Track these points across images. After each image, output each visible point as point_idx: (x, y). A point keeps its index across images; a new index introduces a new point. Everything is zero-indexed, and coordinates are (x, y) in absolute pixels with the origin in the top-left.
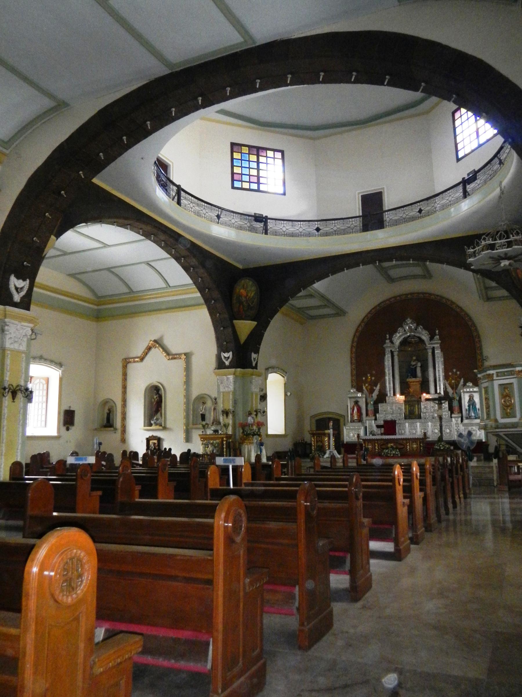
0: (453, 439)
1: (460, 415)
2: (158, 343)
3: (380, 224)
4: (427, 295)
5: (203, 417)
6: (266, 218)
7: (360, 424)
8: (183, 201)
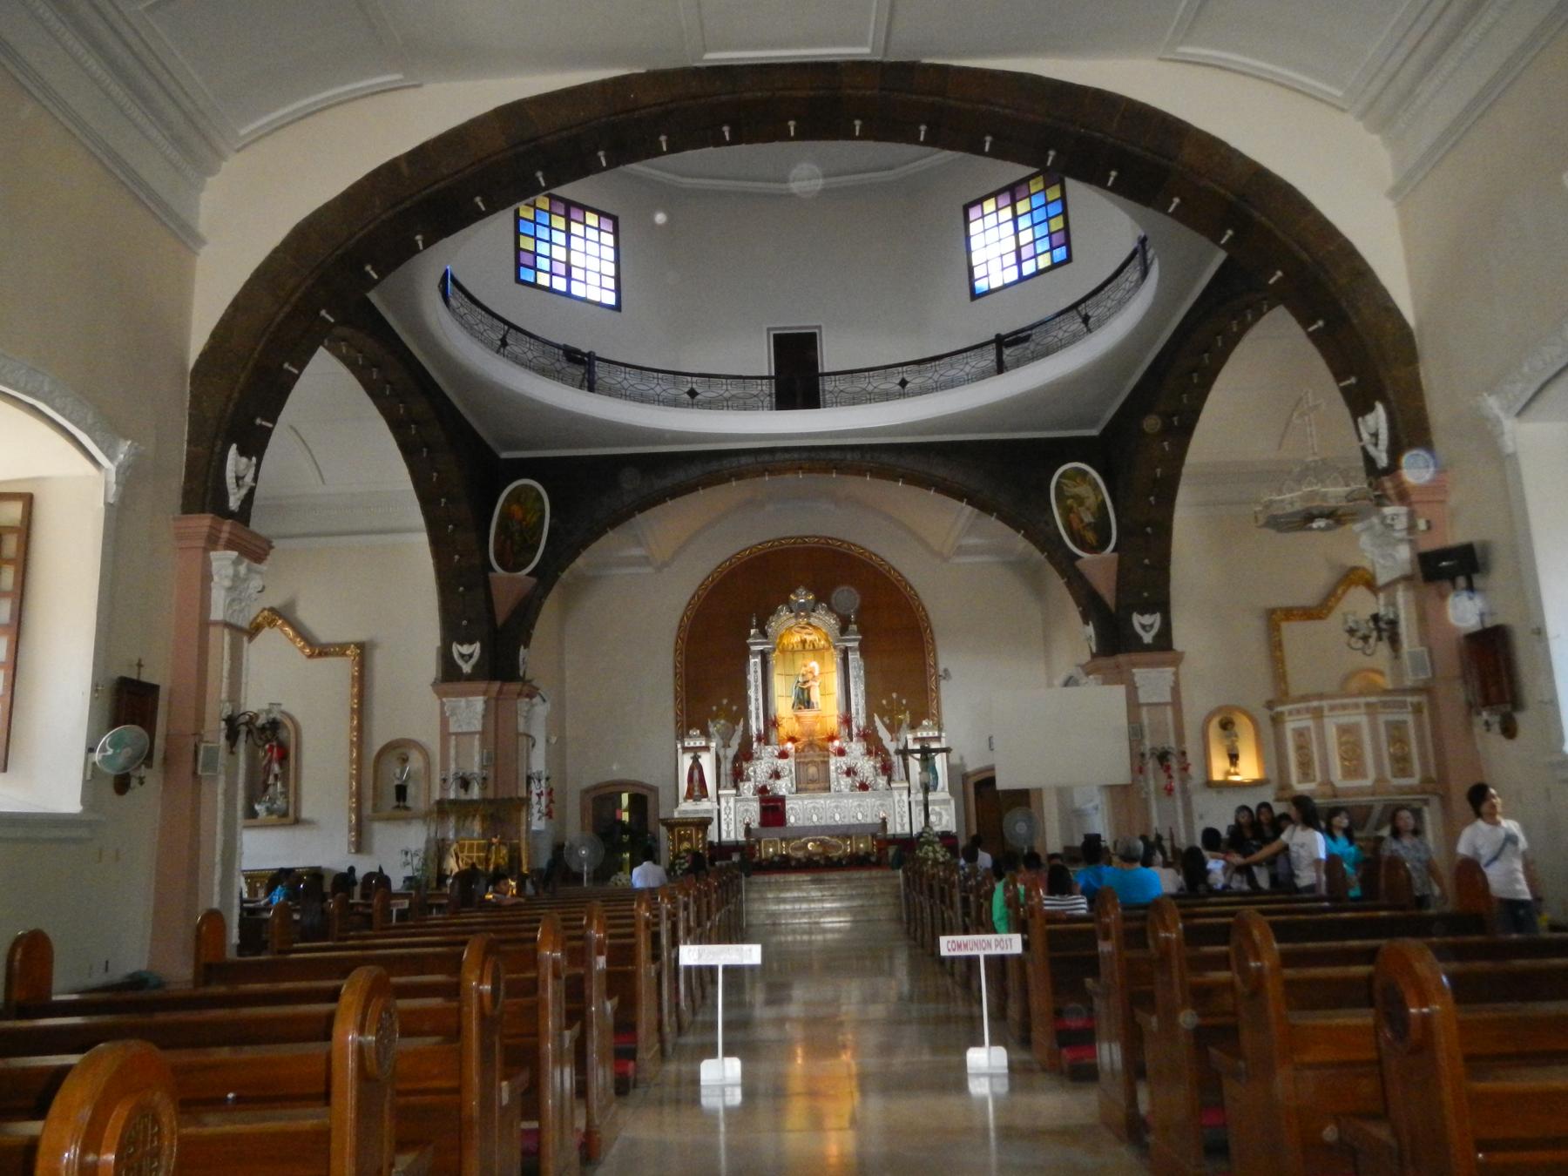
2: (282, 615)
3: (811, 400)
5: (401, 792)
6: (590, 355)
7: (705, 805)
8: (453, 302)
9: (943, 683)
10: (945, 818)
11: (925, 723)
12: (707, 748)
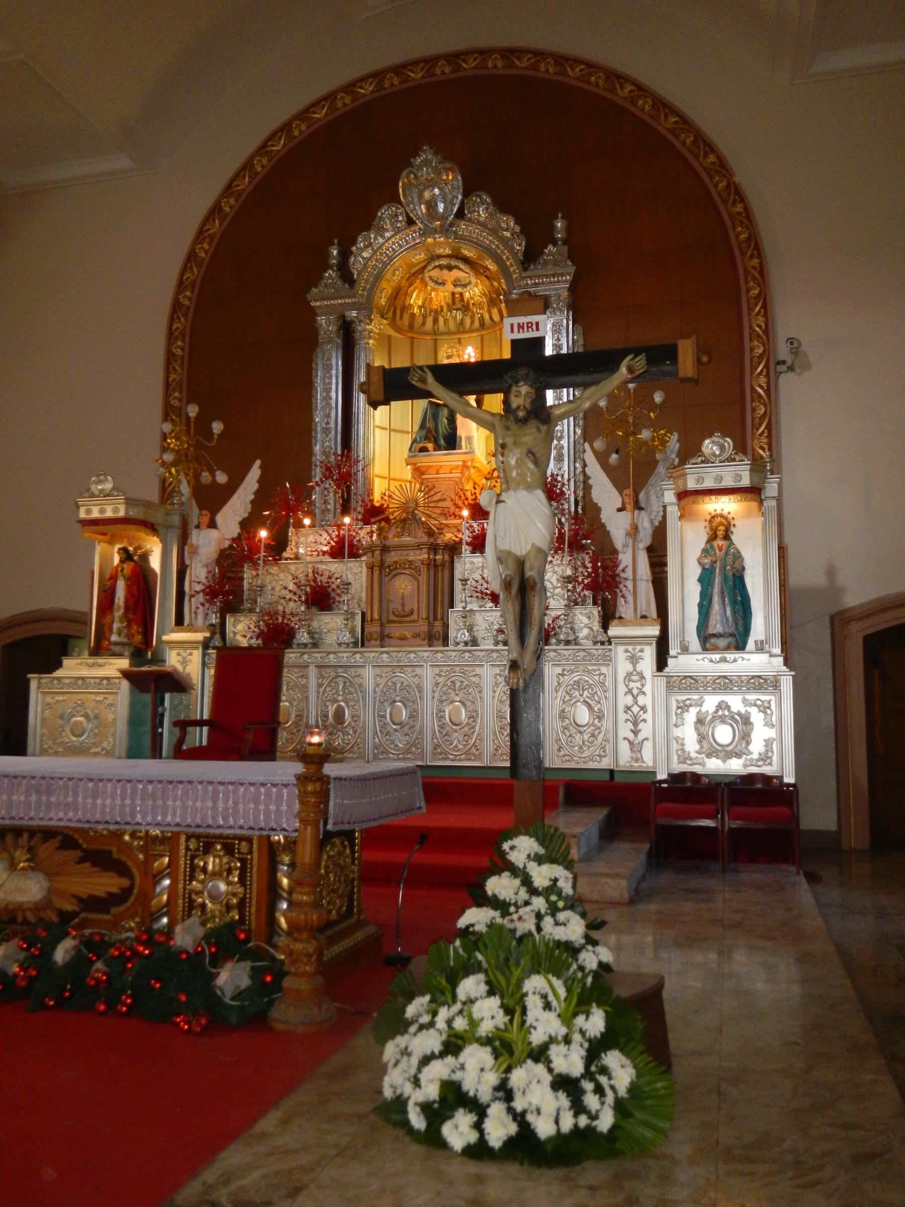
0: (606, 763)
1: (655, 631)
4: (523, 63)
9: (787, 383)
10: (761, 734)
11: (709, 446)
12: (151, 528)
